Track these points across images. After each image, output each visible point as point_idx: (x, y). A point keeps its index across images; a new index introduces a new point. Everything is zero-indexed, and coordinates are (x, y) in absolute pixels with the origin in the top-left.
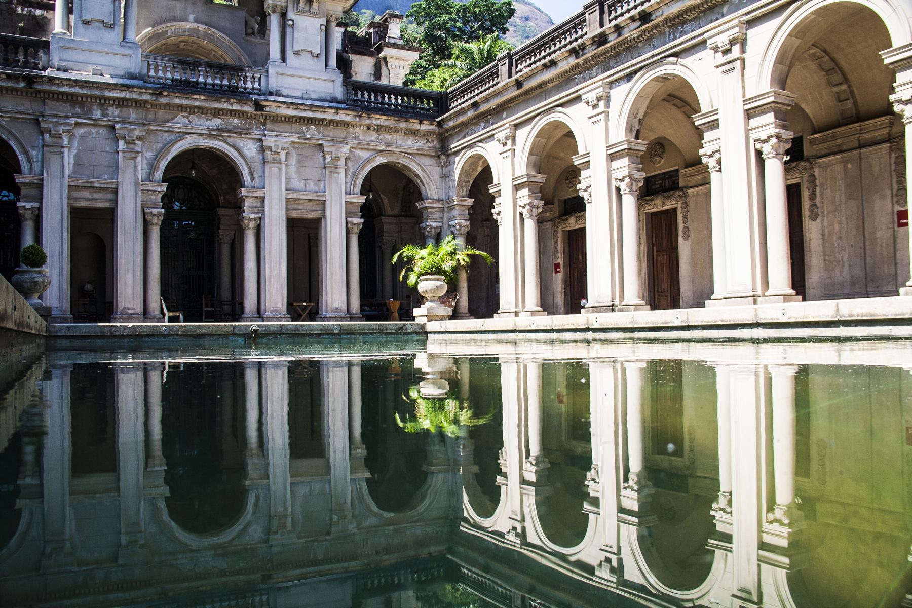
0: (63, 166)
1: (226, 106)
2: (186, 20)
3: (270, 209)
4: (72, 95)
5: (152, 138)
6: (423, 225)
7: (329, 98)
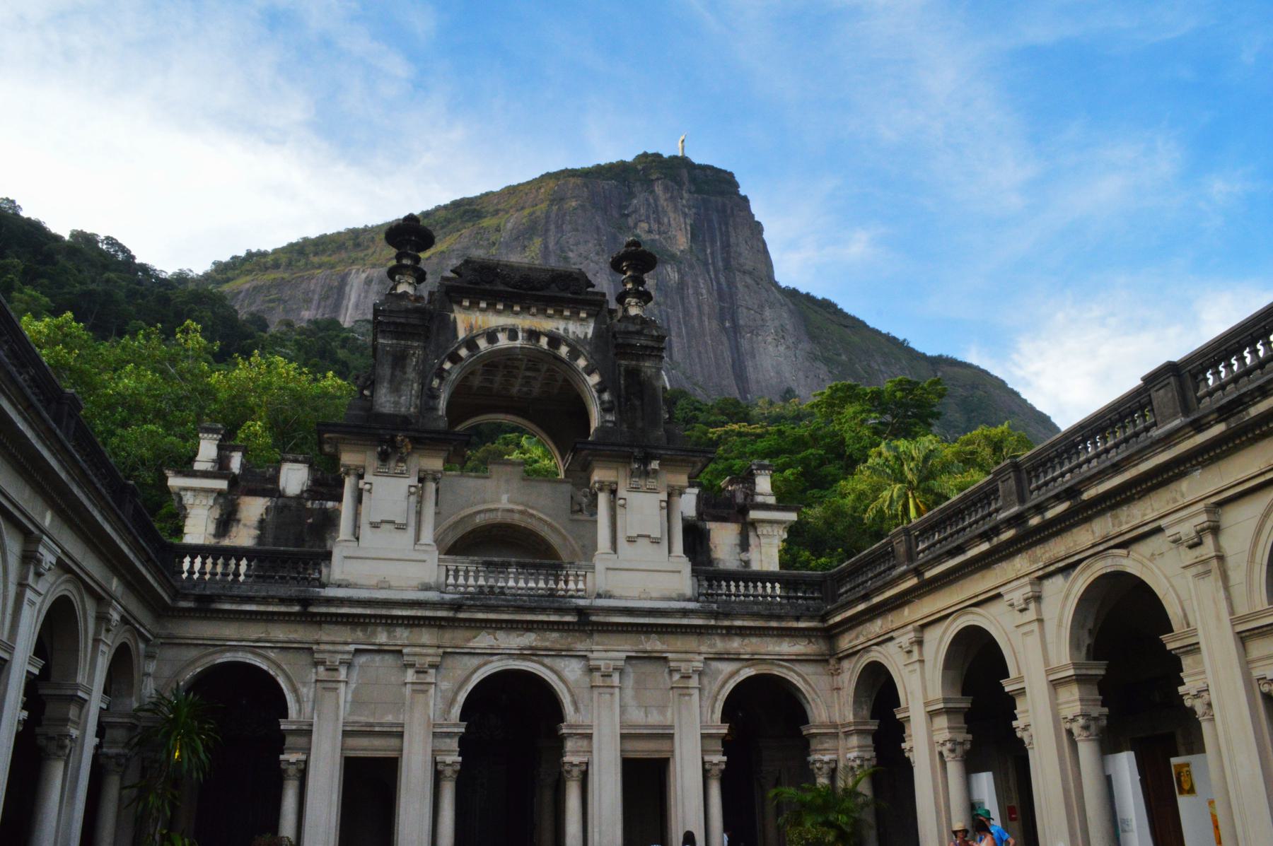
0: (338, 707)
3: (600, 750)
5: (449, 661)
6: (811, 759)
7: (674, 595)
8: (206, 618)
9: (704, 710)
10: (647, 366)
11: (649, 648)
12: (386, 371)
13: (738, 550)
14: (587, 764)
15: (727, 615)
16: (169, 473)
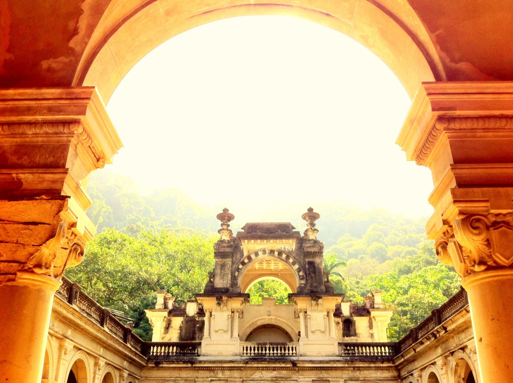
4: (209, 367)
7: (331, 354)
8: (158, 370)
11: (321, 377)
12: (218, 271)
13: (368, 328)
15: (352, 361)
16: (146, 311)
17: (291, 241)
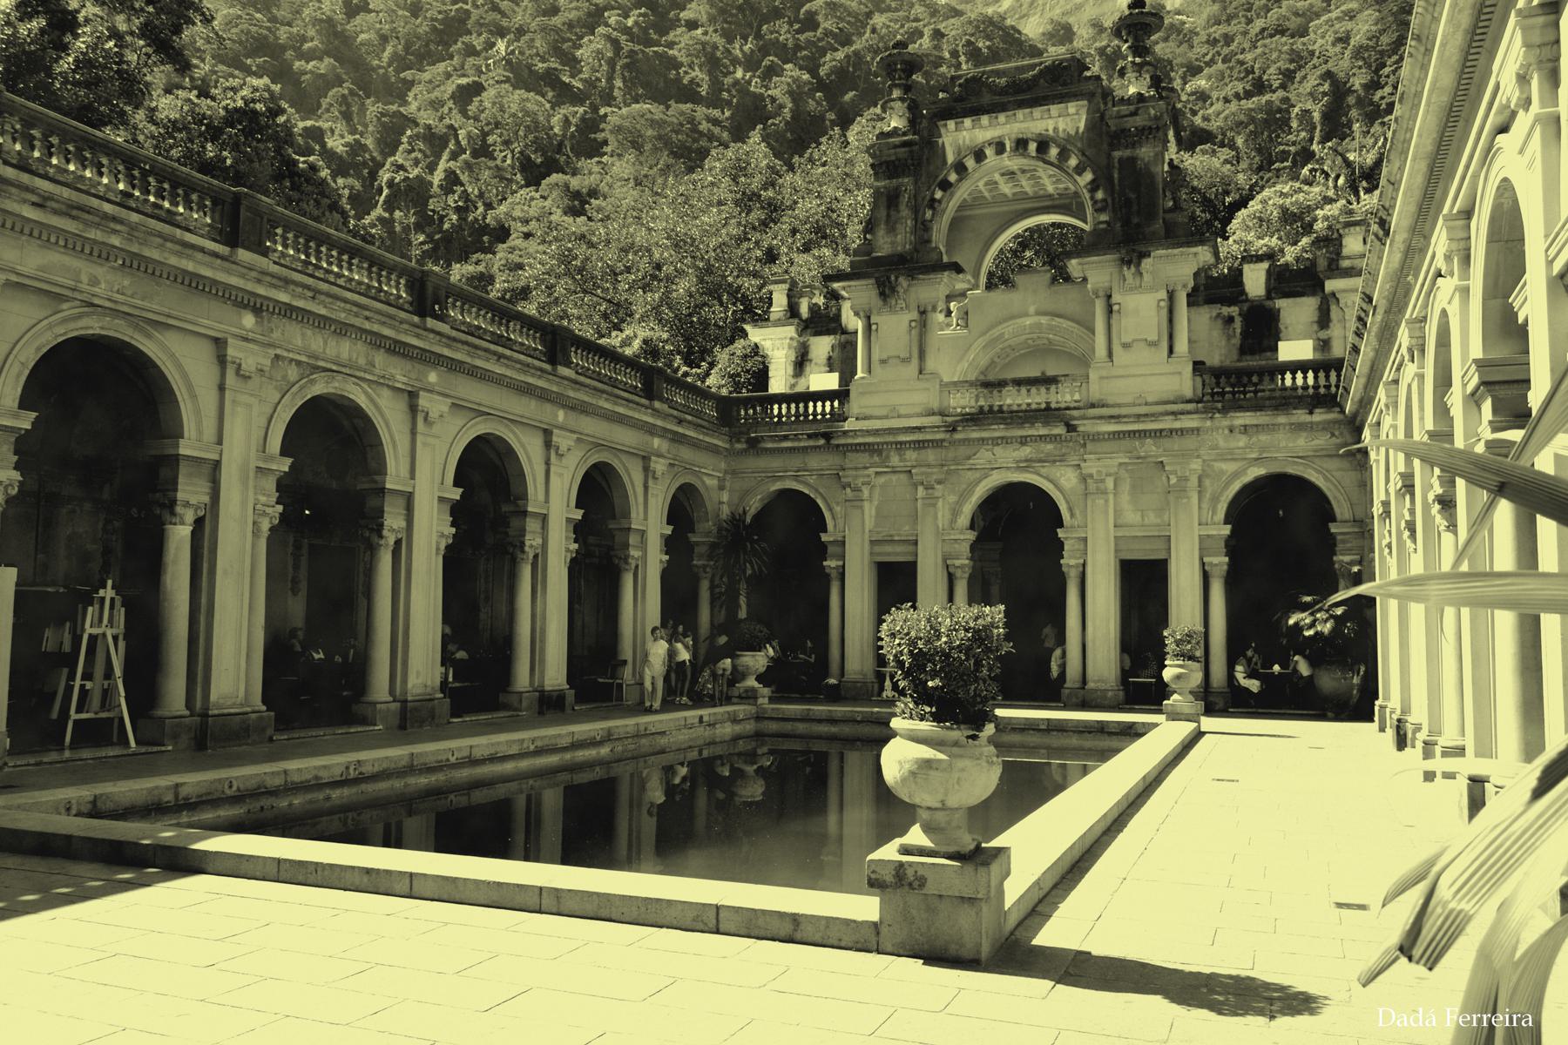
1: (1030, 432)
2: (1026, 315)
9: (1204, 512)
10: (1145, 152)
12: (883, 213)
13: (1315, 327)
14: (1084, 565)
17: (1072, 107)
